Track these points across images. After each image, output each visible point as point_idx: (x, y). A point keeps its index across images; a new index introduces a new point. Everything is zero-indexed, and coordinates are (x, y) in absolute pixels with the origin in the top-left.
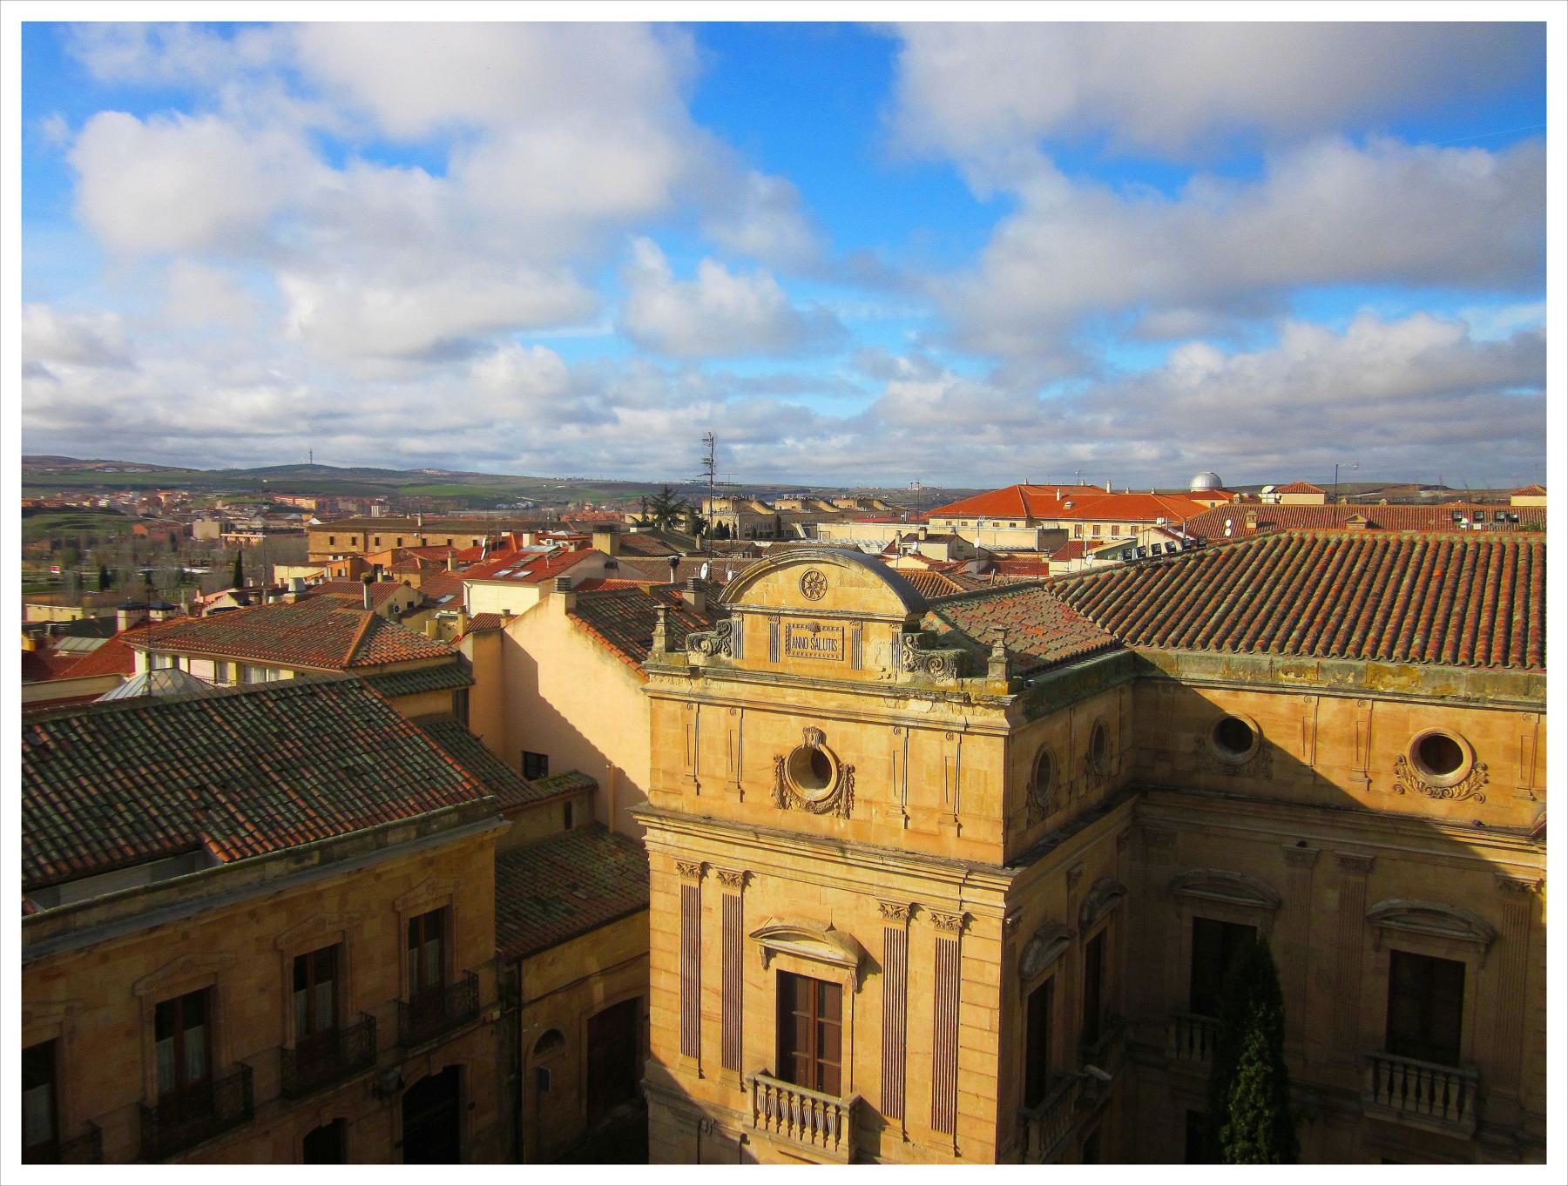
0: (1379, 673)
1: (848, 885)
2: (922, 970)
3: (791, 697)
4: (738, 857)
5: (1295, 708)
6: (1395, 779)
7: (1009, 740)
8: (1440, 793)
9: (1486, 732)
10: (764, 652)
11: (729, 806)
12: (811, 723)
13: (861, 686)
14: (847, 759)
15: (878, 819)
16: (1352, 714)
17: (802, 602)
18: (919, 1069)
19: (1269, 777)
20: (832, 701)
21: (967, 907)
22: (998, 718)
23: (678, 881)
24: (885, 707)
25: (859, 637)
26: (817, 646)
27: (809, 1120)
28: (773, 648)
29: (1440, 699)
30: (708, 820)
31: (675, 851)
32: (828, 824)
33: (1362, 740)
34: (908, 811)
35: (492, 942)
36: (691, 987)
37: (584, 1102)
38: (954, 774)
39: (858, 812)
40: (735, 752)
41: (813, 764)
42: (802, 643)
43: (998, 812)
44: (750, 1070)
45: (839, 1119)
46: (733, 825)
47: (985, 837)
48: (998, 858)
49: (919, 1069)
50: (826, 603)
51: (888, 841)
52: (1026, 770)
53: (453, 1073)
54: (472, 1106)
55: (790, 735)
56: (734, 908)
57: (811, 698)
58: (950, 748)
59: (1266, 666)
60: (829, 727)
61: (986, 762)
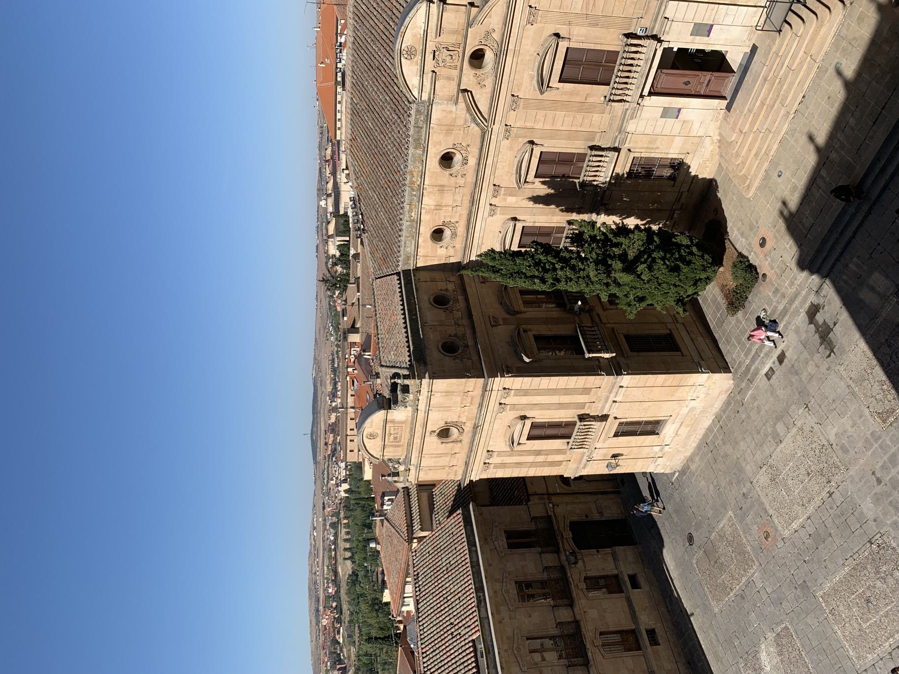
0: (412, 183)
2: (524, 400)
3: (417, 441)
5: (427, 212)
6: (459, 177)
7: (433, 377)
8: (465, 161)
9: (439, 143)
10: (400, 449)
13: (413, 419)
15: (466, 414)
16: (430, 192)
17: (379, 439)
18: (566, 399)
19: (457, 222)
21: (501, 388)
22: (425, 382)
24: (421, 415)
25: (393, 421)
28: (398, 446)
29: (424, 163)
30: (467, 464)
32: (468, 427)
33: (442, 189)
35: (520, 507)
36: (533, 464)
38: (448, 393)
40: (440, 455)
41: (444, 433)
42: (395, 438)
43: (464, 380)
44: (565, 447)
46: (469, 457)
47: (474, 384)
48: (481, 381)
49: (566, 399)
50: (380, 432)
51: (476, 411)
52: (449, 362)
53: (574, 526)
54: (587, 516)
56: (500, 454)
57: (418, 435)
59: (408, 223)
61: (441, 384)
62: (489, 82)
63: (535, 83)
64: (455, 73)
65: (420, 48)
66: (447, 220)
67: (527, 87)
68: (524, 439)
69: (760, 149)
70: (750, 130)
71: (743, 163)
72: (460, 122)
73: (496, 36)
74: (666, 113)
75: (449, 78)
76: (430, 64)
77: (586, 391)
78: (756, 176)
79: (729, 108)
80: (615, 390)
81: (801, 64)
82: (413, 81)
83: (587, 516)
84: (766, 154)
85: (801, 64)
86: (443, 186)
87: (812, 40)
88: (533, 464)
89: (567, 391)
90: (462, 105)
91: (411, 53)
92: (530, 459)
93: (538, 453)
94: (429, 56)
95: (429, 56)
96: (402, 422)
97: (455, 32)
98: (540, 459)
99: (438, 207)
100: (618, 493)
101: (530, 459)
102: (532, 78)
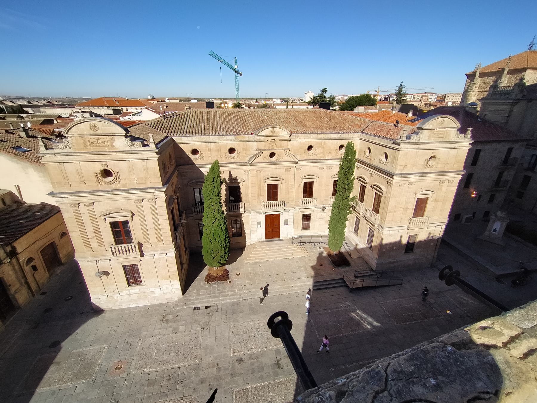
1: (125, 199)
3: (95, 157)
4: (90, 199)
8: (233, 158)
10: (82, 146)
11: (84, 188)
12: (103, 163)
14: (116, 170)
17: (92, 132)
20: (108, 157)
21: (156, 197)
23: (71, 210)
25: (113, 139)
26: (99, 143)
27: (131, 250)
28: (85, 145)
31: (68, 202)
33: (219, 150)
34: (136, 179)
36: (83, 232)
37: (46, 271)
39: (123, 182)
41: (106, 173)
42: (94, 143)
45: (135, 248)
55: (99, 167)
57: (101, 157)
58: (144, 164)
60: (108, 163)
62: (265, 161)
63: (267, 177)
64: (267, 148)
65: (275, 134)
66: (204, 155)
67: (264, 175)
68: (108, 220)
69: (262, 256)
70: (264, 251)
71: (254, 254)
72: (248, 153)
73: (281, 160)
74: (259, 223)
75: (265, 146)
76: (270, 139)
77: (160, 239)
78: (253, 260)
79: (263, 242)
80: (163, 252)
81: (290, 253)
82: (263, 133)
83: (10, 285)
84: (262, 259)
85: (290, 253)
86: (220, 150)
87: (297, 252)
88: (83, 232)
89: (158, 230)
90: (256, 152)
91: (273, 131)
92: (89, 228)
93: (97, 232)
94: (273, 138)
95: (273, 138)
96: (112, 145)
97: (281, 146)
98: (91, 235)
99: (210, 150)
100: (33, 295)
101: (89, 228)
102: (268, 175)
